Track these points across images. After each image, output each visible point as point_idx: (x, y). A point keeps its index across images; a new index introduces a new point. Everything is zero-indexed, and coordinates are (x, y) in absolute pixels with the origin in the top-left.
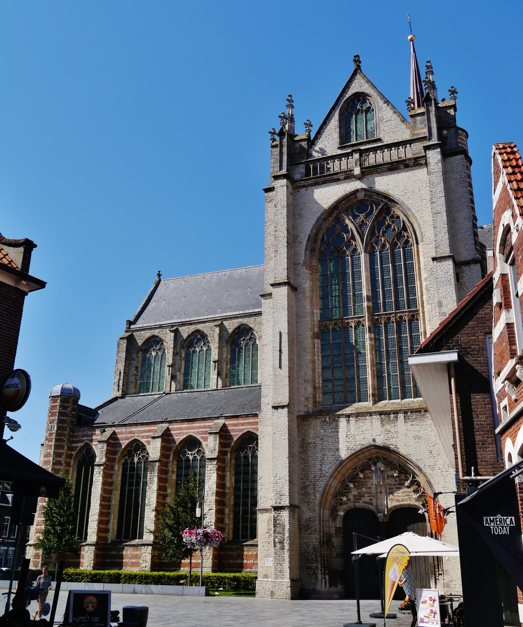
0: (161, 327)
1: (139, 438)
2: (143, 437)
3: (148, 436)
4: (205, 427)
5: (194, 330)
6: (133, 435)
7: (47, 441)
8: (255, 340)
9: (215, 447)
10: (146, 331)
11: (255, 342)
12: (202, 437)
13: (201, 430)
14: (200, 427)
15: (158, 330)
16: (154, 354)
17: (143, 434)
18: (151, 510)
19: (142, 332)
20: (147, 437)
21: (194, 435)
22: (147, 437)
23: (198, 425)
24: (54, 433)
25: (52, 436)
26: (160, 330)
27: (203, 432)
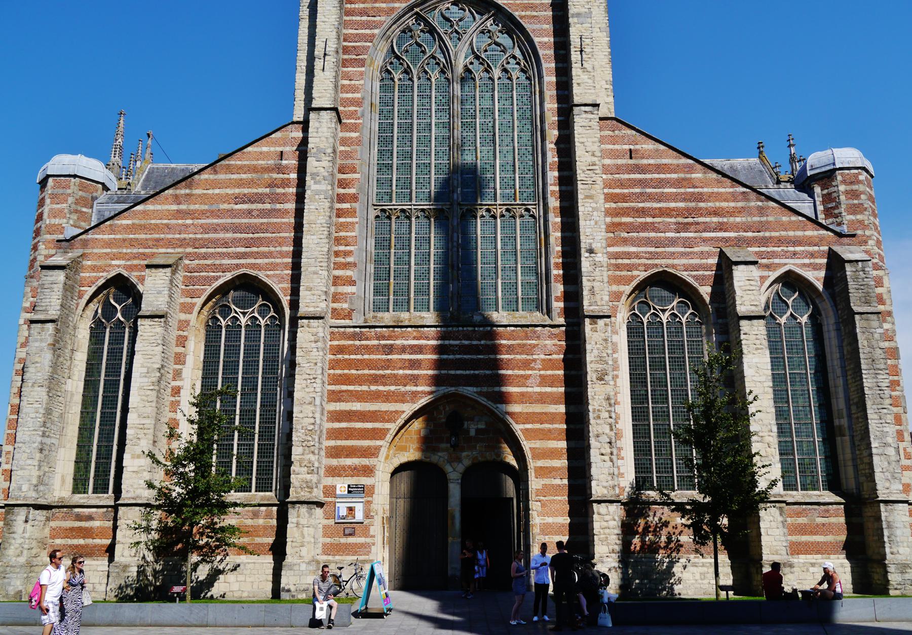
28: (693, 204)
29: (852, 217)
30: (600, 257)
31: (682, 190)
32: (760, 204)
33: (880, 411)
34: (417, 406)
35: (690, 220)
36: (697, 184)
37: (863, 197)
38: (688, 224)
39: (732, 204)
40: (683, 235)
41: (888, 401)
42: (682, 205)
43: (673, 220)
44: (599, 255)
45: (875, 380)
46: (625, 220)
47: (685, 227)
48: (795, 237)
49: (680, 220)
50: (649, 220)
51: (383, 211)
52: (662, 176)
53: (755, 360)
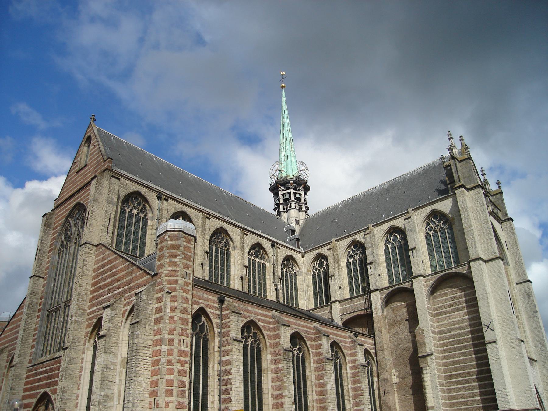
0: (148, 187)
1: (255, 320)
2: (259, 320)
3: (264, 320)
4: (307, 327)
5: (181, 210)
6: (250, 315)
7: (182, 291)
8: (229, 246)
9: (328, 349)
10: (131, 183)
11: (228, 249)
12: (305, 336)
13: (304, 329)
14: (303, 326)
15: (144, 189)
16: (135, 212)
17: (259, 317)
18: (291, 403)
19: (127, 182)
20: (263, 321)
21: (300, 332)
22: (263, 321)
23: (302, 323)
24: (190, 284)
25: (188, 286)
26: (147, 190)
27: (306, 331)
28: (113, 278)
29: (159, 263)
30: (73, 319)
31: (112, 272)
32: (132, 269)
33: (131, 381)
34: (37, 399)
35: (112, 286)
36: (117, 266)
37: (165, 249)
38: (111, 289)
39: (124, 273)
40: (109, 295)
41: (133, 375)
42: (110, 280)
43: (107, 289)
44: (73, 317)
45: (131, 363)
46: (96, 294)
47: (109, 291)
48: (140, 282)
49: (110, 287)
50: (101, 291)
51: (49, 312)
52: (108, 266)
53: (99, 360)
